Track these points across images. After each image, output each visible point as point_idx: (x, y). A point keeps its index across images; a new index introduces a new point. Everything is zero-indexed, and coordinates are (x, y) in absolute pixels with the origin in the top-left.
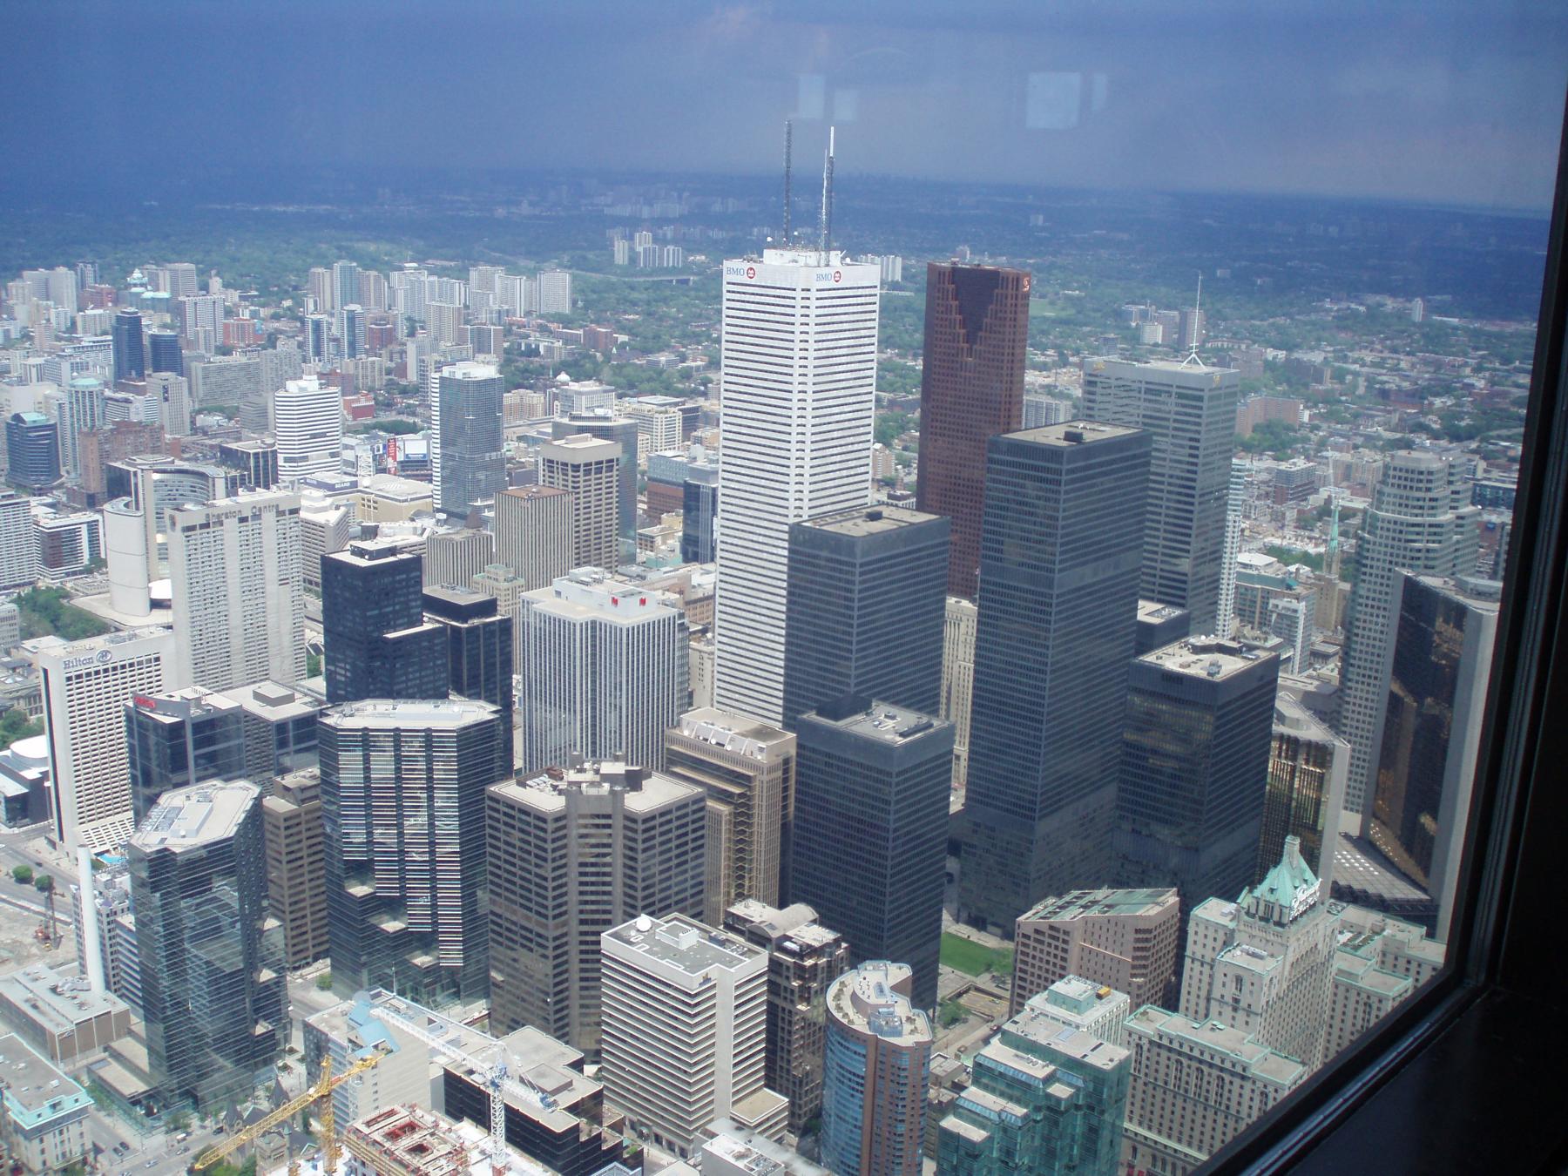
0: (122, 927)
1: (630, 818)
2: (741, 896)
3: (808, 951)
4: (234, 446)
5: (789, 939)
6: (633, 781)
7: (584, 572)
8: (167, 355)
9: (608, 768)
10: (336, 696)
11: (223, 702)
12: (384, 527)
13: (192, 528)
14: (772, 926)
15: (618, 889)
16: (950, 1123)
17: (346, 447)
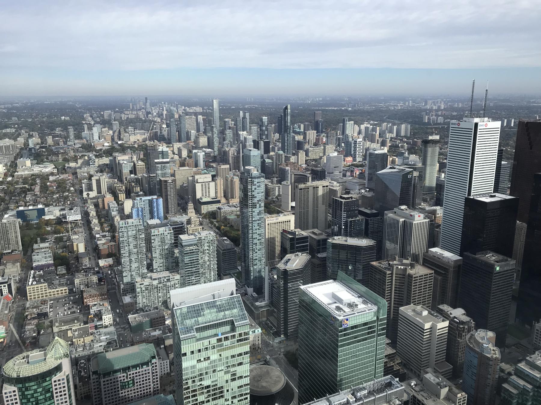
0: (274, 287)
1: (410, 276)
2: (442, 303)
3: (462, 323)
4: (315, 169)
5: (456, 318)
6: (412, 266)
7: (403, 207)
8: (299, 146)
9: (405, 261)
10: (334, 234)
11: (305, 233)
12: (351, 192)
13: (301, 189)
14: (451, 314)
15: (405, 296)
16: (505, 386)
17: (343, 170)
